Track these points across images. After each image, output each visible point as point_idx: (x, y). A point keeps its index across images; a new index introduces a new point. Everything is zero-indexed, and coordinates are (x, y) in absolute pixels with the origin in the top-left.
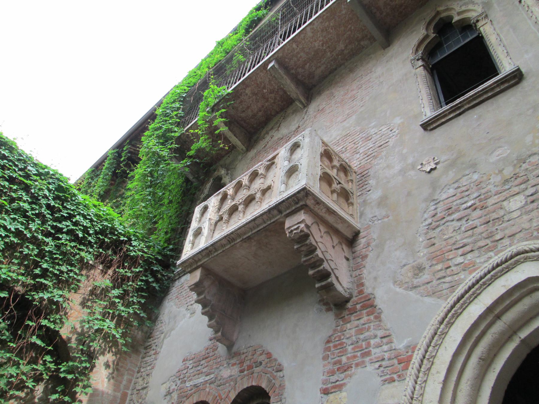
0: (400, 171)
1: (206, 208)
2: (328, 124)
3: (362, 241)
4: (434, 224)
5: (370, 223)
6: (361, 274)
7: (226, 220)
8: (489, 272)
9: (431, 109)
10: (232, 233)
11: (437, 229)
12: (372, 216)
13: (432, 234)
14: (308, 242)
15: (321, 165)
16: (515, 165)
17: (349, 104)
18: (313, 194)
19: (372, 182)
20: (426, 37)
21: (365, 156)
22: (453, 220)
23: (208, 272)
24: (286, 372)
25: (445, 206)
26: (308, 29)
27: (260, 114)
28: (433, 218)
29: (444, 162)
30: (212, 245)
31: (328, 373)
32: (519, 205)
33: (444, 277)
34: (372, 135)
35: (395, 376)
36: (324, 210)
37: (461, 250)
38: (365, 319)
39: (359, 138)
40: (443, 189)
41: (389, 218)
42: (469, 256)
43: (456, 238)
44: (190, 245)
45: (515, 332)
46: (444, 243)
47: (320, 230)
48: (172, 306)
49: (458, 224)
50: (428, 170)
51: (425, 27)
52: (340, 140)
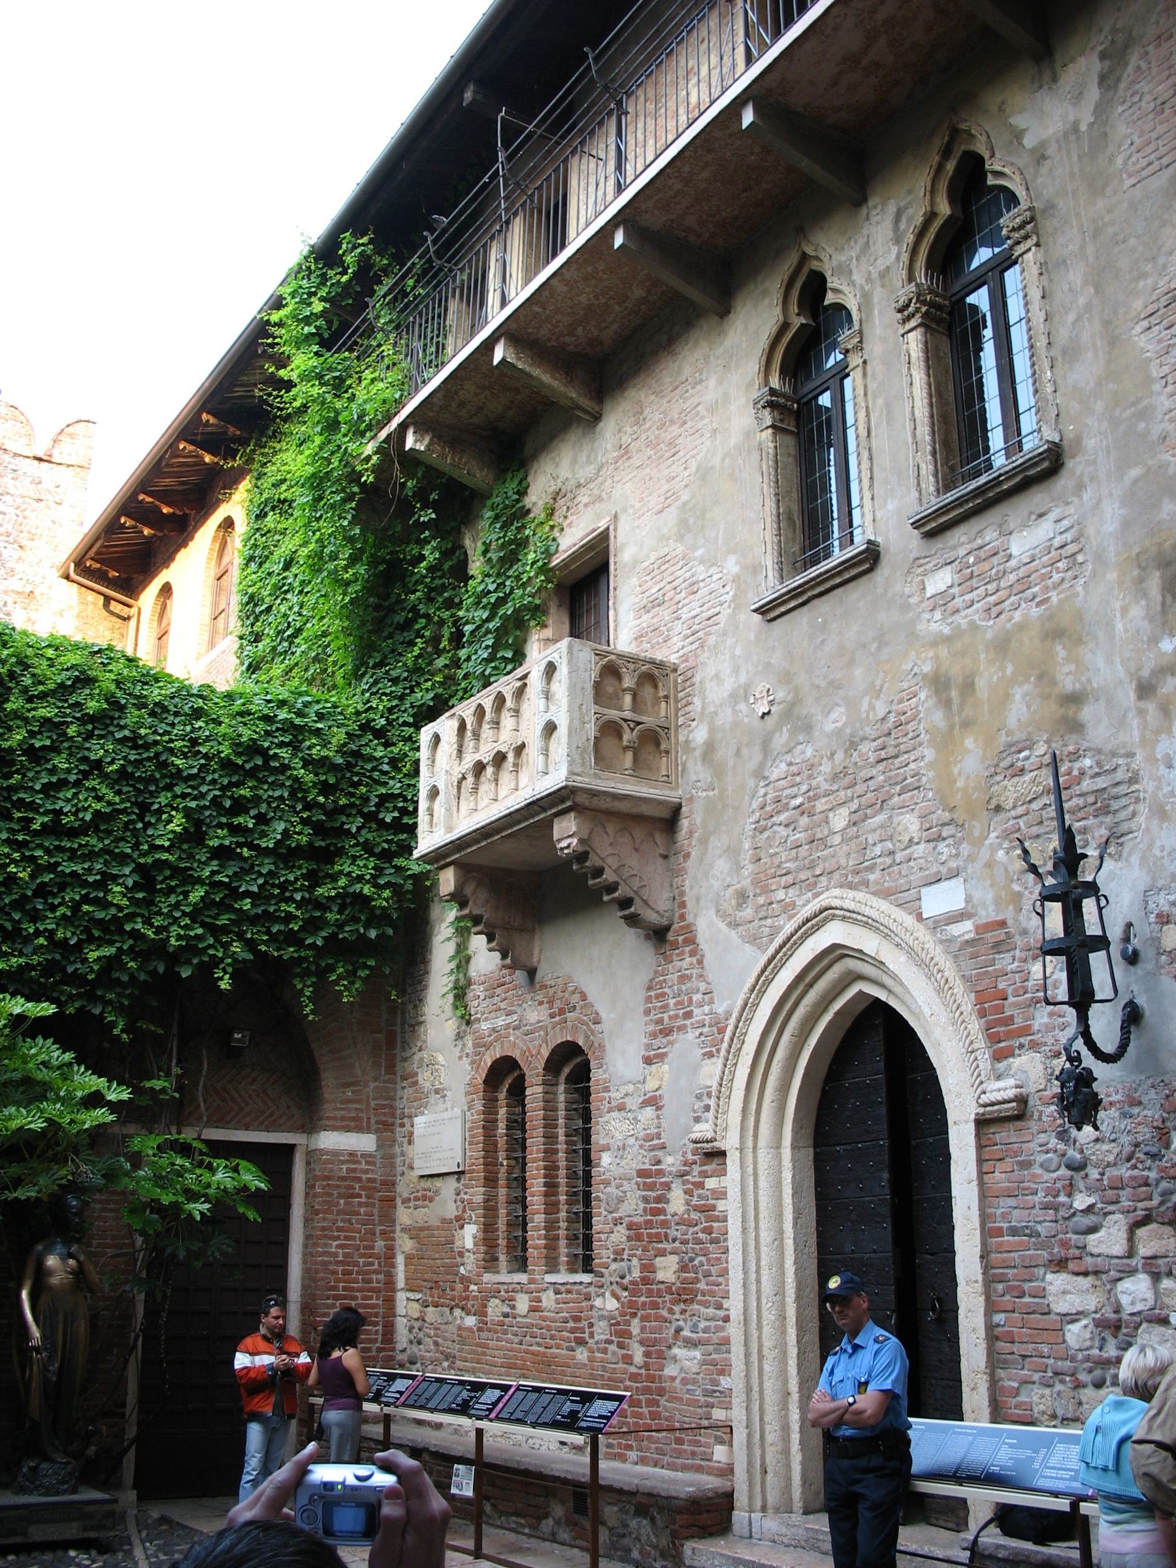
0: (732, 696)
1: (437, 739)
2: (637, 505)
3: (684, 823)
4: (762, 823)
8: (800, 928)
10: (483, 827)
12: (694, 778)
14: (587, 864)
16: (846, 751)
17: (667, 463)
18: (582, 789)
20: (784, 327)
23: (465, 869)
24: (605, 1026)
26: (554, 282)
27: (511, 413)
30: (458, 839)
31: (650, 1035)
32: (843, 824)
33: (766, 918)
34: (698, 582)
35: (714, 1049)
36: (608, 800)
37: (784, 878)
38: (688, 960)
39: (681, 579)
42: (791, 891)
44: (427, 818)
45: (831, 1002)
49: (783, 831)
51: (780, 301)
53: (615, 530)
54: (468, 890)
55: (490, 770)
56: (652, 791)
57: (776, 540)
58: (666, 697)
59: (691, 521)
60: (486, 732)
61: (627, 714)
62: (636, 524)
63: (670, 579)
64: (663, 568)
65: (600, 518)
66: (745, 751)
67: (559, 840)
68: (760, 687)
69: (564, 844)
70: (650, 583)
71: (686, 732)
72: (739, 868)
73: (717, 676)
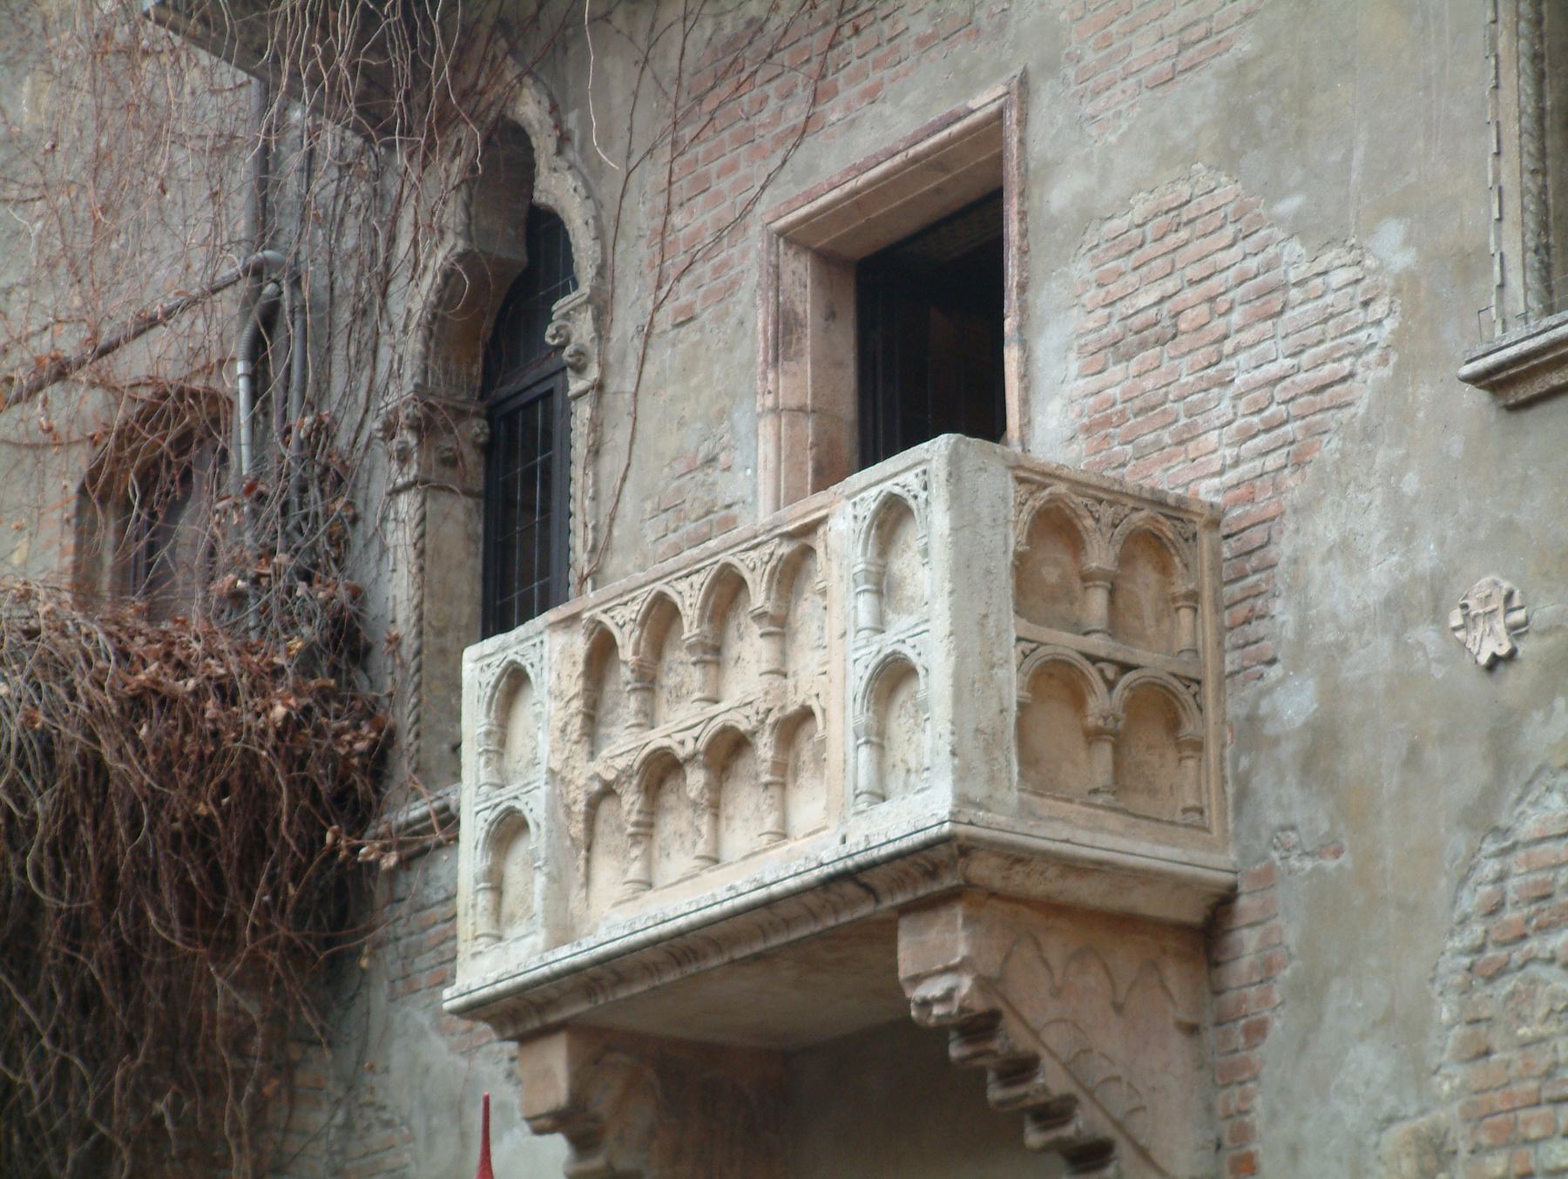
1: (515, 680)
2: (1091, 58)
3: (1247, 941)
4: (1490, 953)
5: (1275, 855)
6: (1246, 1112)
7: (637, 824)
9: (1525, 251)
10: (680, 934)
11: (1498, 983)
12: (1275, 818)
13: (1482, 992)
14: (996, 1045)
15: (1019, 639)
19: (1283, 612)
21: (1256, 419)
22: (1551, 960)
25: (1531, 878)
28: (1490, 920)
29: (1543, 633)
34: (1284, 286)
36: (1052, 872)
39: (1231, 273)
40: (1530, 782)
41: (1343, 858)
43: (1555, 1049)
44: (484, 900)
46: (1515, 1055)
47: (1045, 962)
48: (422, 1034)
50: (1484, 659)
52: (1148, 226)
53: (1023, 122)
54: (603, 1102)
55: (696, 779)
56: (1163, 851)
57: (1532, 185)
58: (1193, 597)
59: (1264, 115)
60: (682, 670)
61: (1098, 644)
62: (1088, 109)
63: (1193, 272)
64: (1172, 240)
65: (970, 84)
66: (1436, 757)
67: (917, 980)
68: (1484, 586)
69: (934, 989)
70: (1132, 278)
71: (1248, 692)
72: (1419, 1072)
73: (1345, 548)
